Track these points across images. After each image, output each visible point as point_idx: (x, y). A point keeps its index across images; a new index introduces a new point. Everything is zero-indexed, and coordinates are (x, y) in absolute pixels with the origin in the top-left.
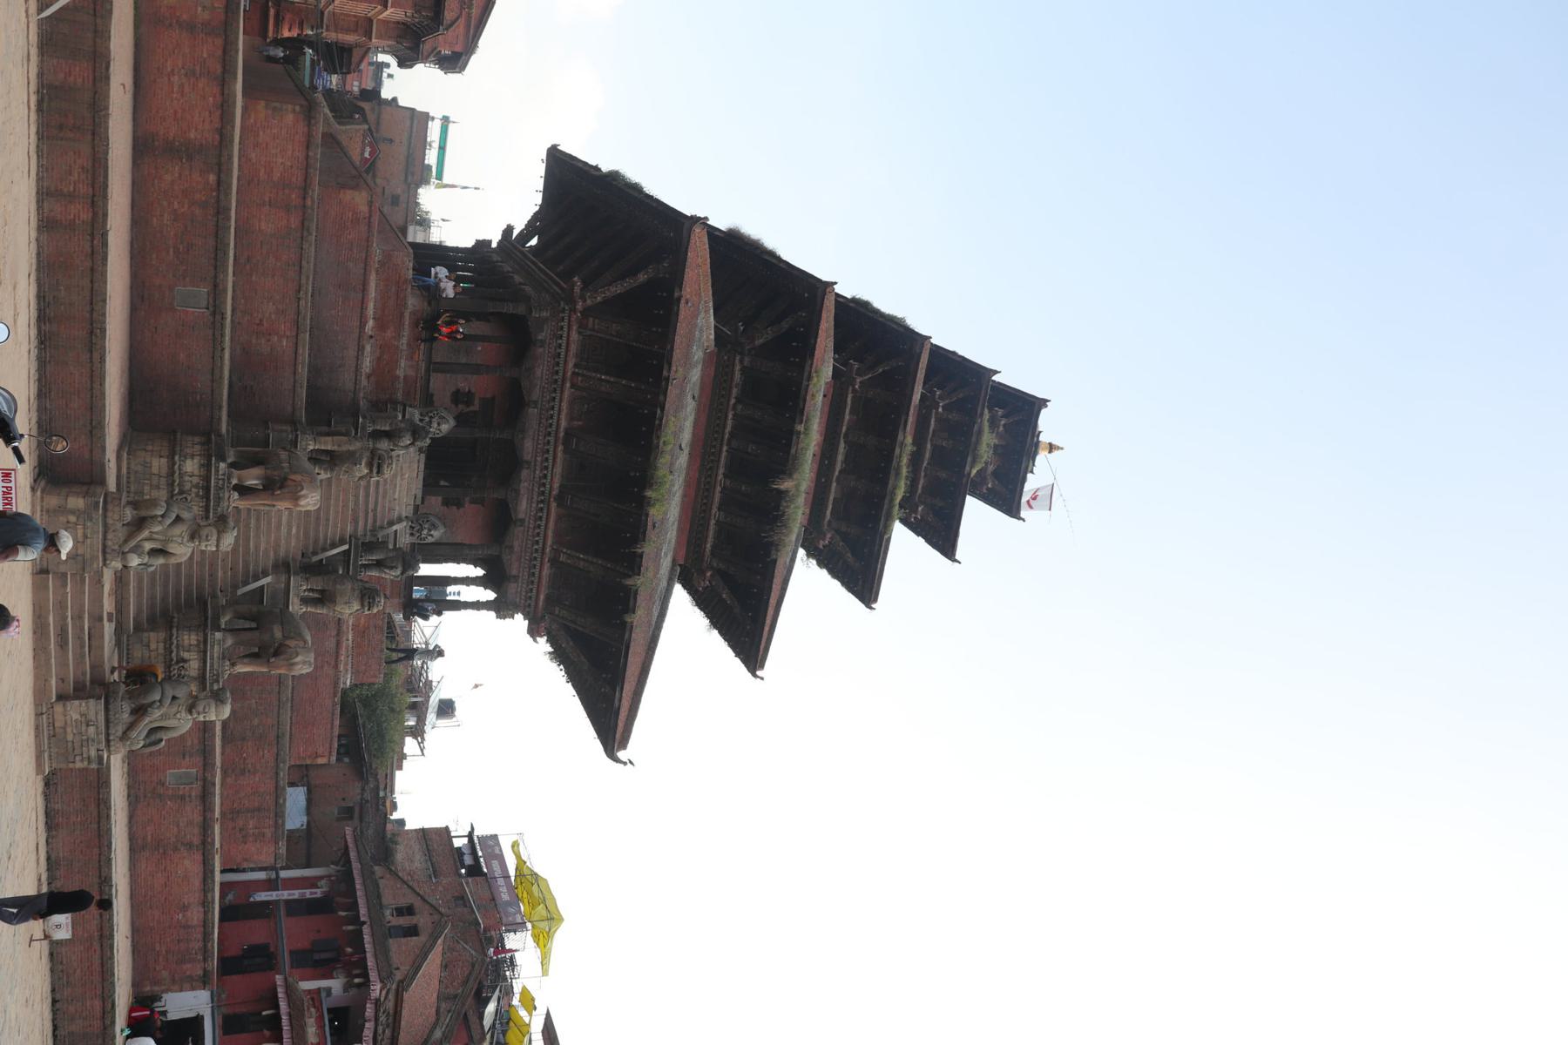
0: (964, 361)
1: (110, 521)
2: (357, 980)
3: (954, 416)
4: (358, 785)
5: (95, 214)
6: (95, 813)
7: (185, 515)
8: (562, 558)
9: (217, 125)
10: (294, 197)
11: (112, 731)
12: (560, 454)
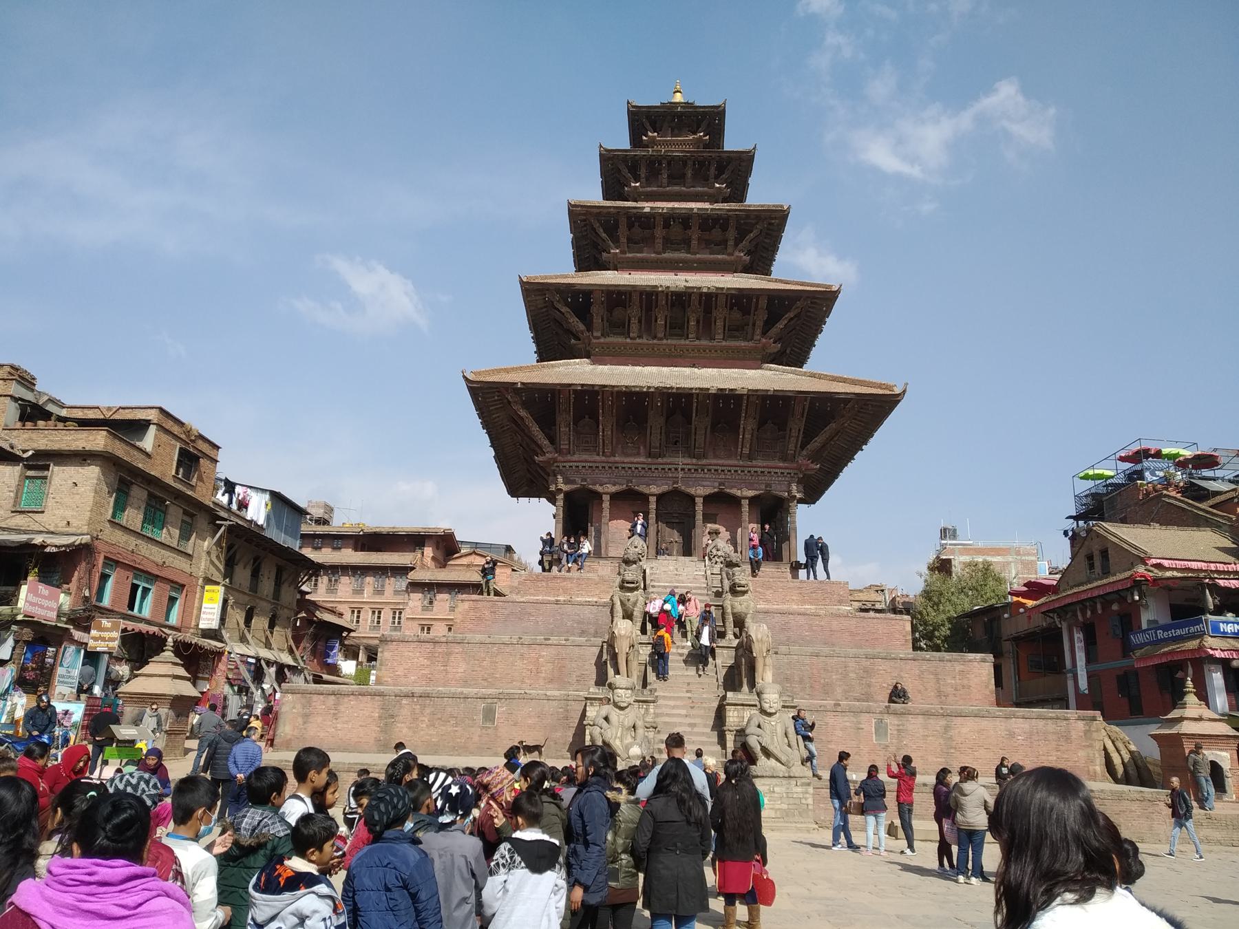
0: (604, 174)
3: (643, 172)
7: (603, 713)
10: (441, 649)
12: (665, 460)
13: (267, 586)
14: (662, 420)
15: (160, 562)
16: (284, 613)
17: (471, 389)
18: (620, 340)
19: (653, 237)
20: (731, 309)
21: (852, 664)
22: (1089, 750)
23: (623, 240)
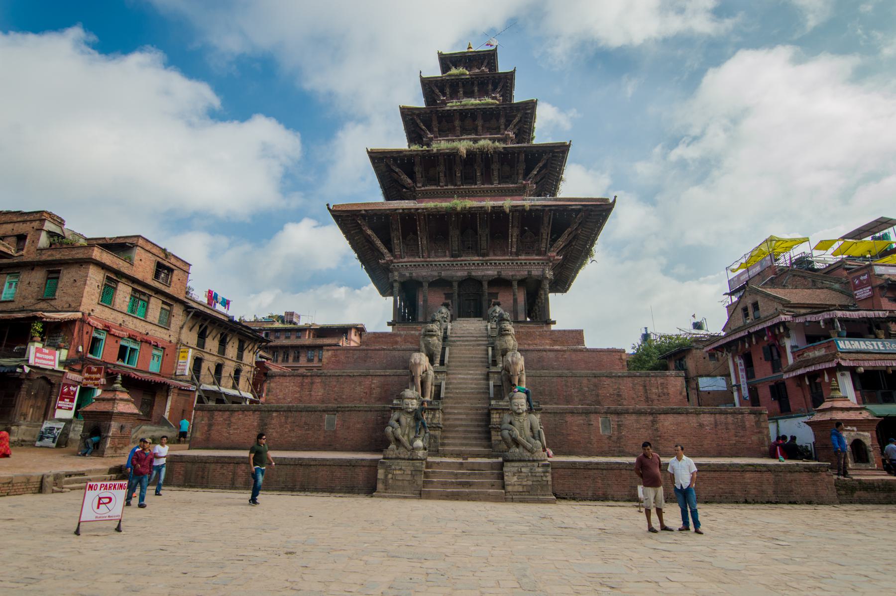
1: (394, 456)
2: (782, 330)
3: (448, 91)
4: (694, 351)
5: (243, 462)
6: (595, 471)
8: (514, 250)
9: (251, 413)
11: (527, 458)
13: (232, 350)
14: (458, 232)
15: (144, 332)
16: (245, 369)
17: (334, 216)
18: (433, 187)
19: (454, 127)
20: (502, 165)
21: (585, 381)
22: (760, 435)
23: (436, 129)
